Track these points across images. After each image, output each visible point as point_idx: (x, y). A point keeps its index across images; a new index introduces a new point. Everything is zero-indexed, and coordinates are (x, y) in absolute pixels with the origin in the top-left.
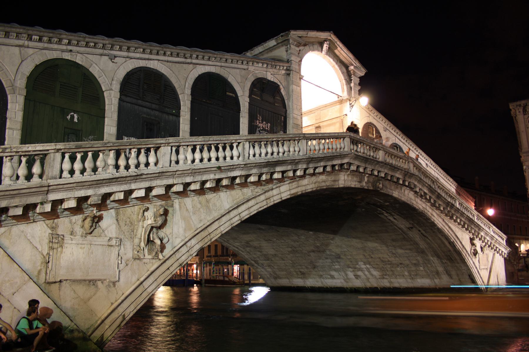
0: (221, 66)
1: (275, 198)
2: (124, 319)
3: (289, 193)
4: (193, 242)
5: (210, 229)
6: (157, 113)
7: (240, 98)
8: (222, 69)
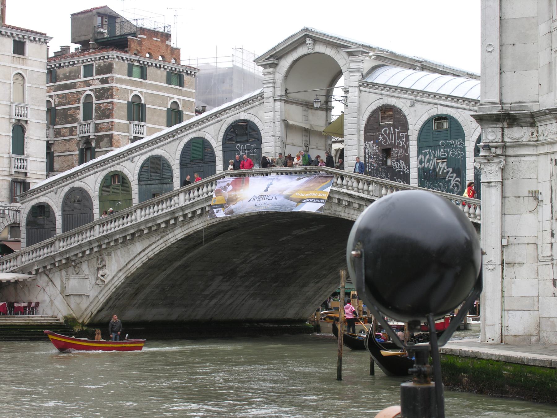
0: (199, 130)
1: (171, 240)
2: (92, 314)
3: (182, 234)
4: (120, 274)
5: (129, 266)
6: (160, 185)
7: (215, 150)
8: (201, 132)
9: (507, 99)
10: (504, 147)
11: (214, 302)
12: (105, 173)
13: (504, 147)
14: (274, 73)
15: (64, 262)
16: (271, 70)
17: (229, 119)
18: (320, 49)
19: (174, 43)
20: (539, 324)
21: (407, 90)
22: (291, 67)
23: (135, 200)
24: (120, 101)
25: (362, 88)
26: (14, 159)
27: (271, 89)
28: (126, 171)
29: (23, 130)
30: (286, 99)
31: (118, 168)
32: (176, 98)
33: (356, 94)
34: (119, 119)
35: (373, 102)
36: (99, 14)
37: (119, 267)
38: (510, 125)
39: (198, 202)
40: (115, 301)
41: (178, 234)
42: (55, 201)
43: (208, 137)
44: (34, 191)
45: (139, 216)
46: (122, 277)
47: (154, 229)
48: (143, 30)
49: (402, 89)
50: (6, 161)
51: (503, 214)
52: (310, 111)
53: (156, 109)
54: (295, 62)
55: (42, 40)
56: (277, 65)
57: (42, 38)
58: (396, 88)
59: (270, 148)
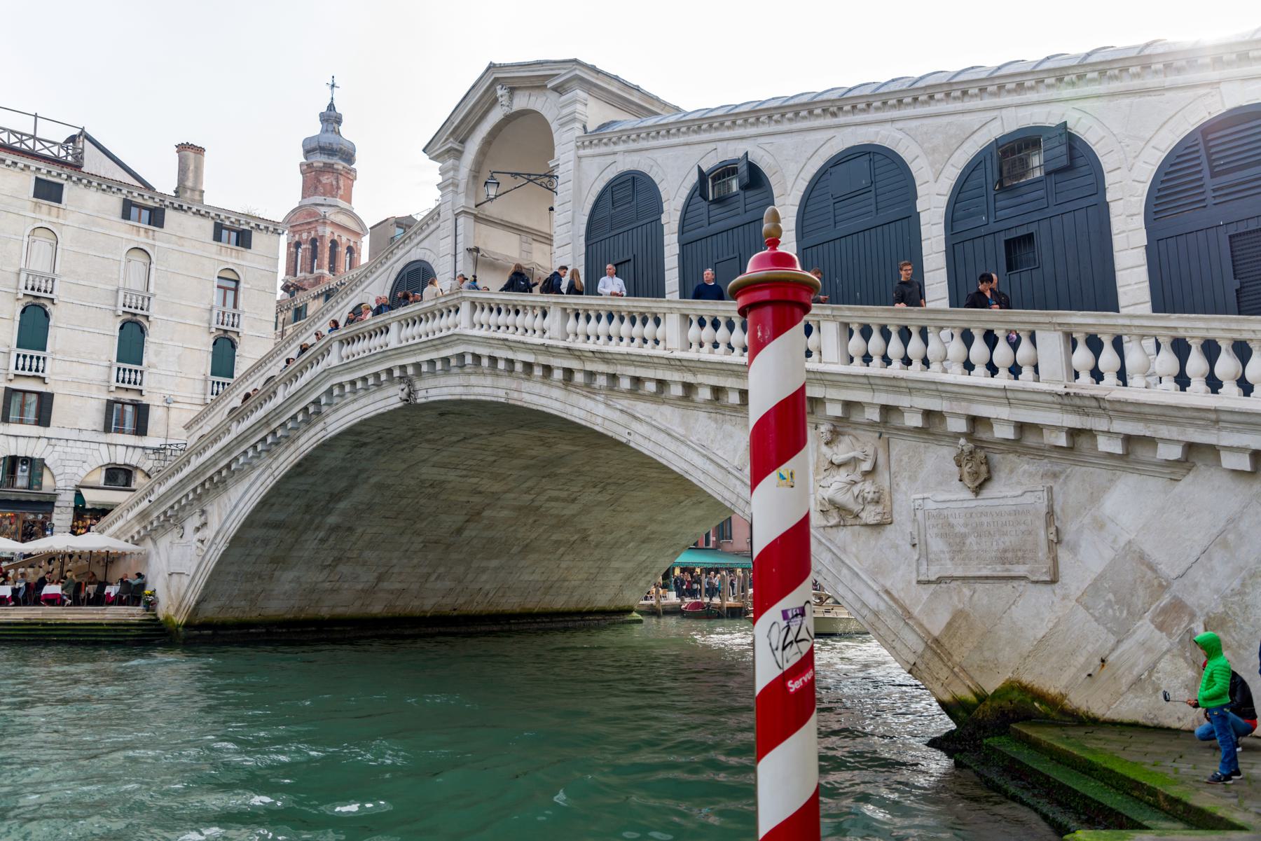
14: (456, 169)
15: (162, 518)
16: (450, 162)
18: (522, 102)
25: (582, 152)
26: (210, 383)
27: (449, 197)
33: (571, 165)
50: (199, 386)
52: (536, 245)
55: (271, 229)
56: (461, 153)
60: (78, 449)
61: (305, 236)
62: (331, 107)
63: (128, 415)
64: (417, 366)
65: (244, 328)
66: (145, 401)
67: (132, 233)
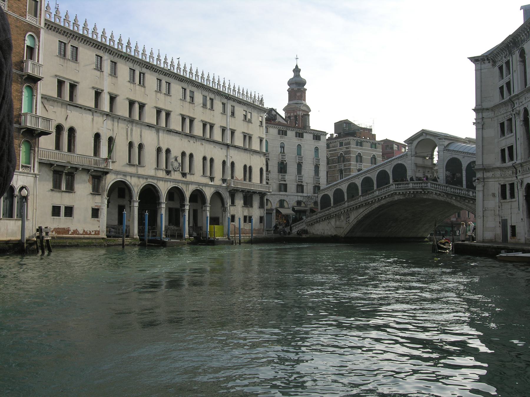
9: (484, 163)
10: (484, 179)
11: (389, 230)
12: (349, 183)
13: (484, 179)
17: (395, 163)
18: (428, 137)
19: (373, 133)
20: (495, 236)
21: (461, 152)
22: (417, 144)
23: (360, 194)
24: (353, 156)
28: (356, 183)
29: (318, 167)
30: (416, 155)
31: (353, 181)
32: (374, 153)
34: (353, 162)
35: (448, 156)
36: (345, 123)
37: (354, 217)
38: (486, 172)
39: (383, 194)
40: (352, 230)
41: (376, 205)
42: (331, 194)
43: (387, 170)
44: (322, 190)
45: (362, 199)
46: (356, 221)
47: (367, 204)
48: (362, 128)
49: (460, 152)
50: (312, 179)
51: (483, 200)
53: (367, 158)
54: (419, 142)
57: (325, 134)
58: (458, 151)
59: (409, 173)
60: (292, 197)
61: (292, 114)
62: (297, 66)
63: (300, 188)
64: (417, 192)
65: (321, 163)
66: (303, 184)
67: (296, 141)
